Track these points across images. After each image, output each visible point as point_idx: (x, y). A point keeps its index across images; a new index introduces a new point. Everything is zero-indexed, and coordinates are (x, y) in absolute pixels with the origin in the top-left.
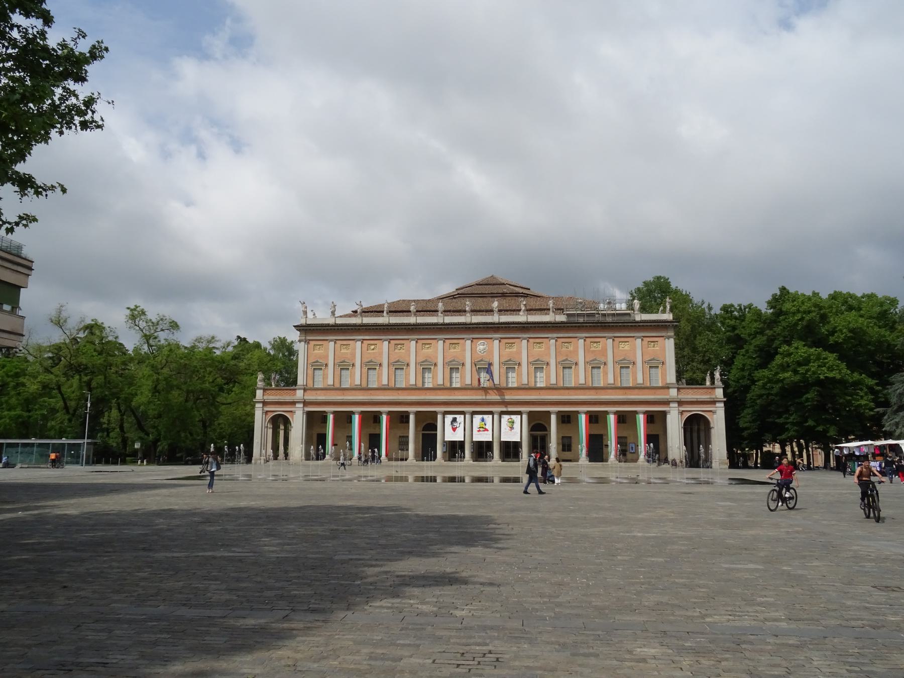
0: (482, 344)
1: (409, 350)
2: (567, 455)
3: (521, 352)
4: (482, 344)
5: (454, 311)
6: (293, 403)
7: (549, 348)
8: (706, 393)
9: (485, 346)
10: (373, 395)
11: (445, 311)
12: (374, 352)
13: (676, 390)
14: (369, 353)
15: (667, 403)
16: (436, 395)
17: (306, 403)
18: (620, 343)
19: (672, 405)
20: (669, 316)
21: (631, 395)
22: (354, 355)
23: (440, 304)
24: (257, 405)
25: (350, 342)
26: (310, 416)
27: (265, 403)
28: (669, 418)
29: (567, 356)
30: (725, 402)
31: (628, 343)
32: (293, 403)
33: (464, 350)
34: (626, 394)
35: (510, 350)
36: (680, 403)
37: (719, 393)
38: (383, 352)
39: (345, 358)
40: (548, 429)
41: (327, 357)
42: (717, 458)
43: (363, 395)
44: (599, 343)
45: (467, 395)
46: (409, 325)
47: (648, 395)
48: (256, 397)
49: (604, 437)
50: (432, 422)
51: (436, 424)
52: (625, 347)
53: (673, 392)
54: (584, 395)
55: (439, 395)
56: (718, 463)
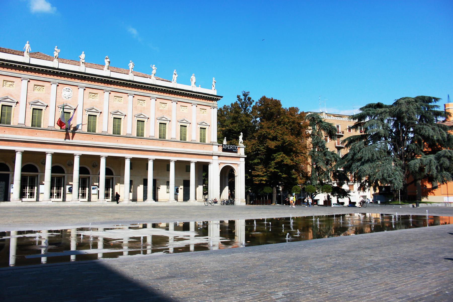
0: (68, 90)
4: (68, 90)
9: (70, 92)
13: (217, 146)
16: (16, 134)
18: (181, 107)
21: (188, 148)
28: (210, 168)
29: (141, 111)
30: (245, 158)
31: (186, 108)
33: (49, 94)
37: (241, 152)
40: (114, 173)
42: (239, 198)
44: (166, 104)
45: (49, 137)
52: (185, 110)
54: (154, 145)
55: (19, 134)
56: (240, 201)
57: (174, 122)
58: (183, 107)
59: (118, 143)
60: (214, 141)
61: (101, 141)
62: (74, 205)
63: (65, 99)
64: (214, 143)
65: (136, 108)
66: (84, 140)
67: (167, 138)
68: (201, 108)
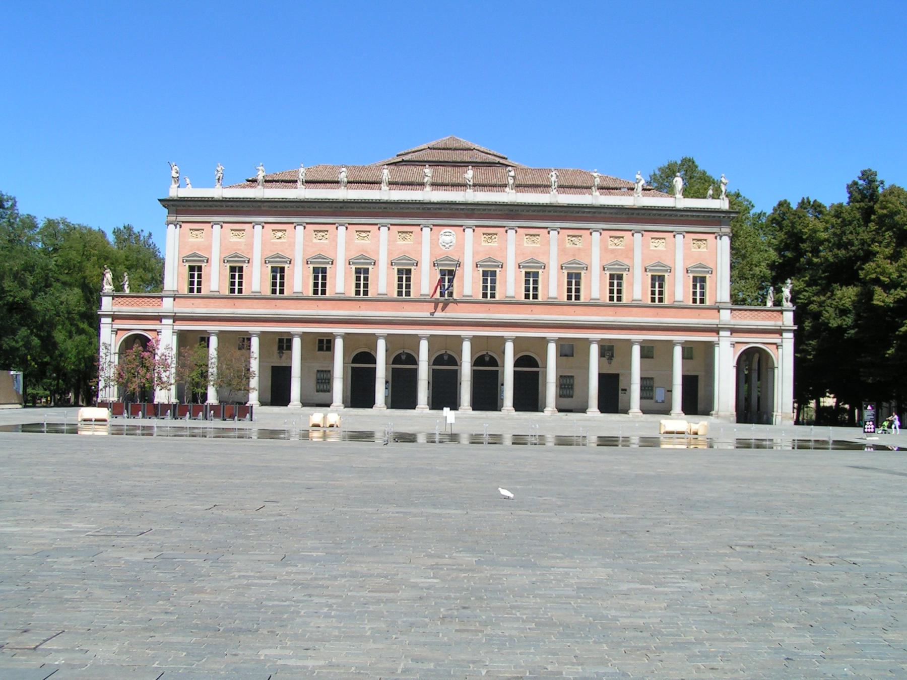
0: (448, 234)
1: (335, 240)
2: (567, 402)
3: (506, 248)
4: (448, 234)
5: (403, 184)
6: (159, 318)
7: (548, 243)
8: (769, 318)
10: (278, 308)
11: (390, 183)
12: (281, 243)
14: (273, 244)
15: (716, 330)
17: (176, 318)
18: (653, 240)
19: (722, 333)
20: (724, 204)
22: (250, 246)
23: (386, 172)
24: (103, 320)
25: (247, 227)
26: (183, 338)
27: (114, 317)
29: (574, 255)
31: (663, 240)
32: (159, 318)
33: (420, 243)
34: (657, 315)
35: (489, 244)
36: (733, 331)
38: (294, 243)
39: (239, 250)
41: (209, 248)
43: (264, 308)
46: (336, 202)
47: (691, 318)
48: (102, 308)
49: (621, 378)
50: (367, 350)
51: (373, 353)
52: (661, 246)
53: (726, 316)
54: (597, 315)
57: (638, 271)
58: (657, 241)
59: (533, 314)
60: (723, 301)
61: (503, 313)
62: (460, 415)
63: (444, 248)
64: (721, 304)
66: (477, 313)
67: (625, 299)
68: (694, 238)
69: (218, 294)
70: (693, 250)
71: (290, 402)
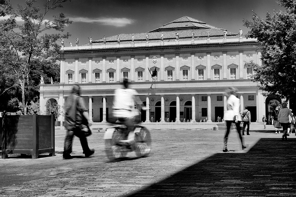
0: (155, 58)
4: (155, 58)
12: (98, 64)
14: (96, 65)
39: (84, 68)
65: (197, 62)
69: (78, 83)
70: (247, 58)
71: (102, 120)
